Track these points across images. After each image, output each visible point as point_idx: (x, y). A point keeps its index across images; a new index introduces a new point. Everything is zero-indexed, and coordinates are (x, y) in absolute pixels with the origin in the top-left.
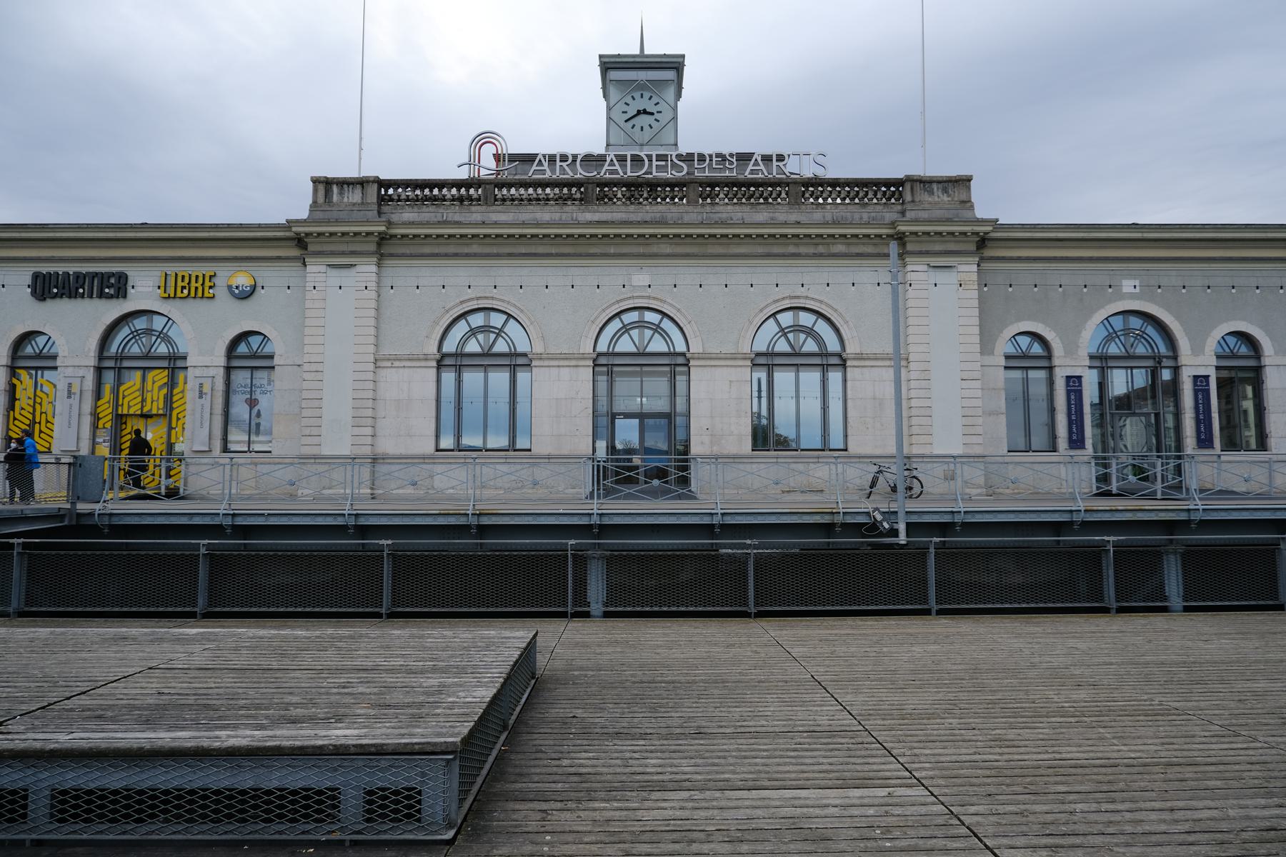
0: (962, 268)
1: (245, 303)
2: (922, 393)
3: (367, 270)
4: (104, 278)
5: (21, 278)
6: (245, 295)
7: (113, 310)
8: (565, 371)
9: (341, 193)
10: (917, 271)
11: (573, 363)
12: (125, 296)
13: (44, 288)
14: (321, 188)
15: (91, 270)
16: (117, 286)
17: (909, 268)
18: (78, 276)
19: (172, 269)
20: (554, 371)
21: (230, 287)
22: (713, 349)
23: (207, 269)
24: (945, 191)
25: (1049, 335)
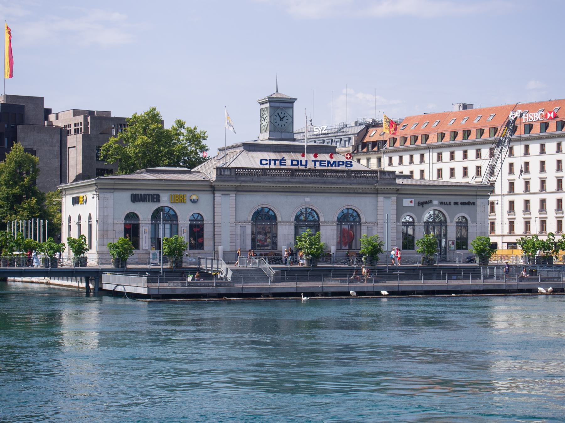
0: (393, 198)
1: (192, 204)
2: (381, 234)
3: (233, 196)
4: (153, 196)
5: (126, 196)
6: (194, 202)
7: (154, 206)
8: (287, 226)
9: (224, 171)
10: (381, 199)
11: (289, 224)
12: (159, 202)
13: (135, 199)
14: (218, 169)
15: (148, 193)
16: (156, 199)
17: (379, 198)
18: (145, 195)
19: (173, 193)
20: (284, 226)
21: (191, 200)
22: (327, 220)
23: (181, 193)
24: (389, 175)
25: (414, 216)
